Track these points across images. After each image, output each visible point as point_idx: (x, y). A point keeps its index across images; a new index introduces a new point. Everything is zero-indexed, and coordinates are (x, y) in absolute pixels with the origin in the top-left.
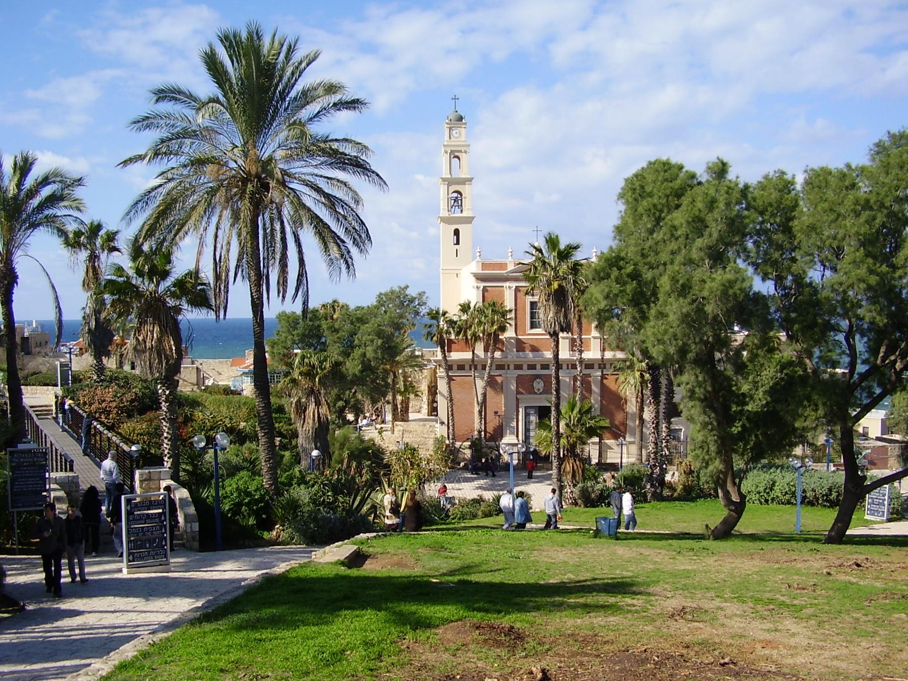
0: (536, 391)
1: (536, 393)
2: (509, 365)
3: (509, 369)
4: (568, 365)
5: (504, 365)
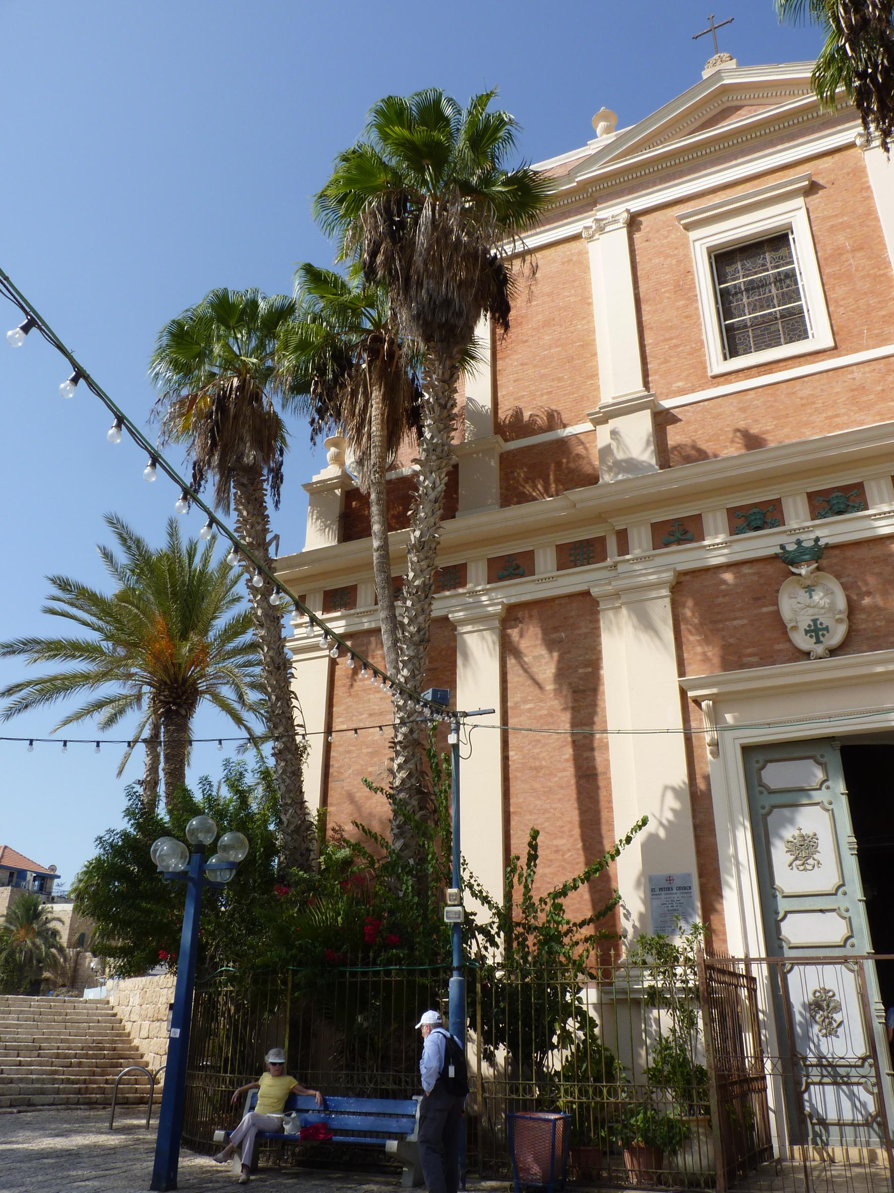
0: (803, 642)
1: (807, 655)
2: (623, 537)
3: (623, 549)
5: (602, 540)
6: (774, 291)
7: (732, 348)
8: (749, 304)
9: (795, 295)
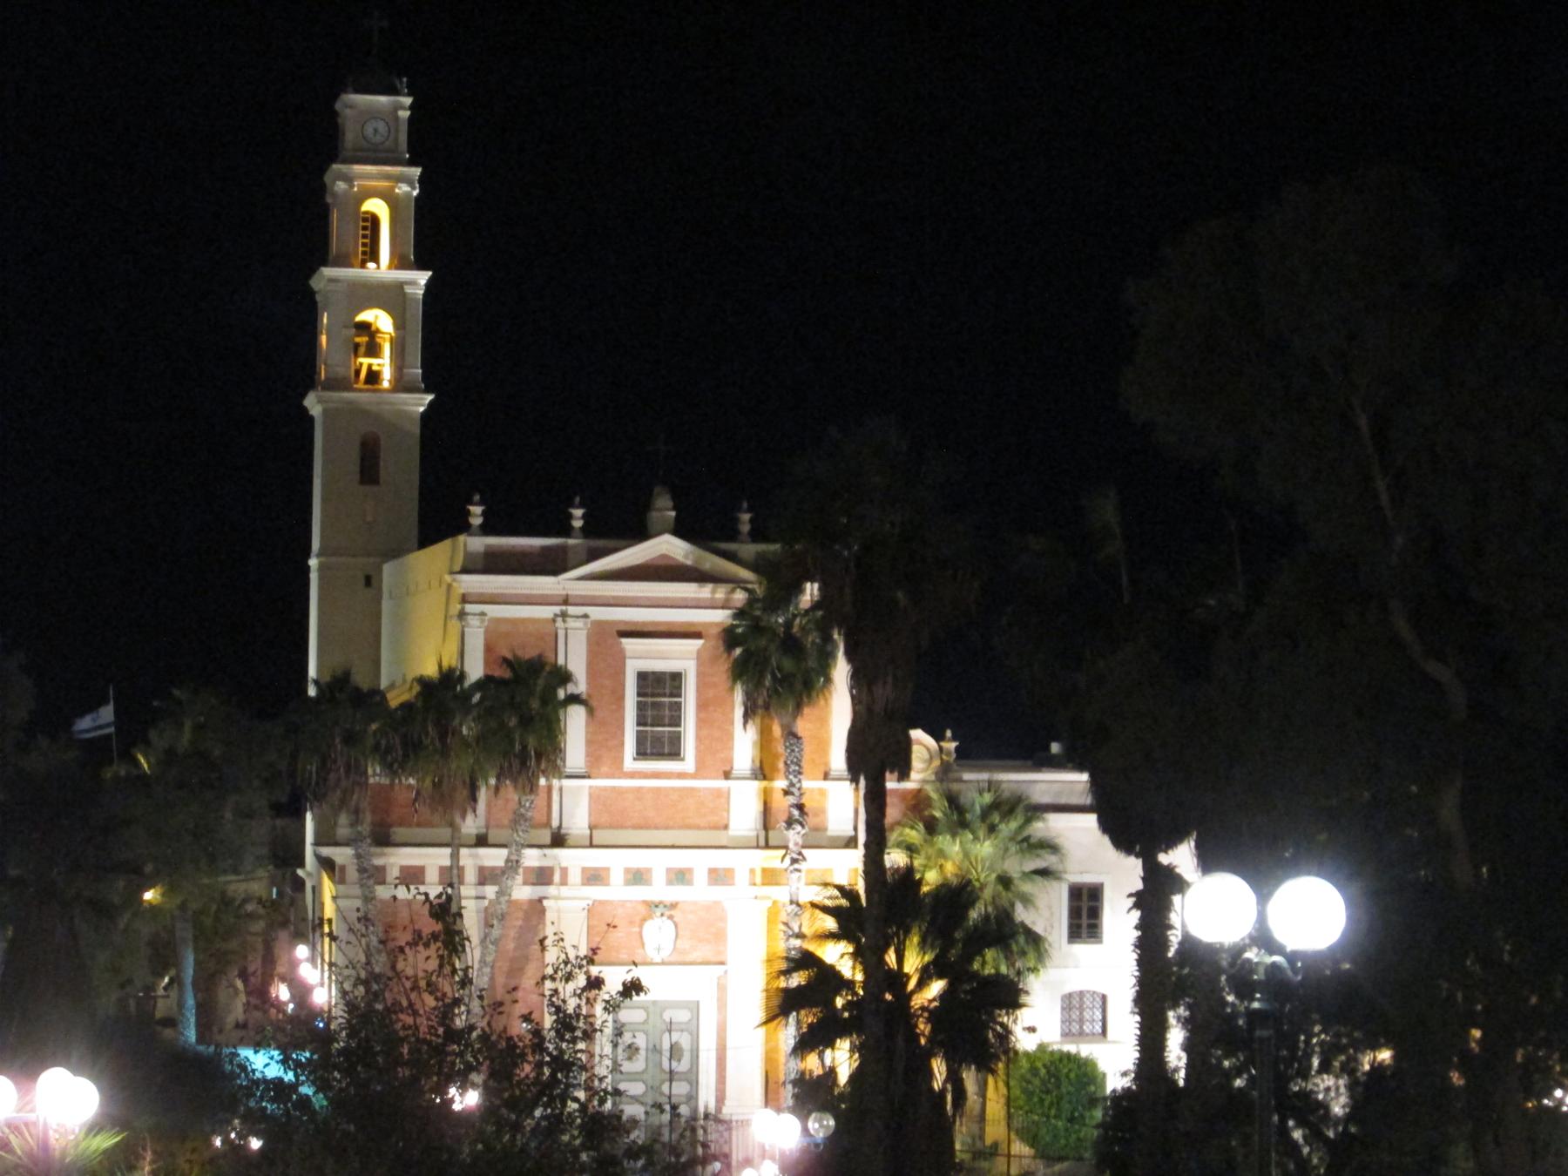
2: (564, 871)
4: (752, 871)
6: (667, 712)
7: (641, 754)
8: (652, 715)
9: (676, 721)
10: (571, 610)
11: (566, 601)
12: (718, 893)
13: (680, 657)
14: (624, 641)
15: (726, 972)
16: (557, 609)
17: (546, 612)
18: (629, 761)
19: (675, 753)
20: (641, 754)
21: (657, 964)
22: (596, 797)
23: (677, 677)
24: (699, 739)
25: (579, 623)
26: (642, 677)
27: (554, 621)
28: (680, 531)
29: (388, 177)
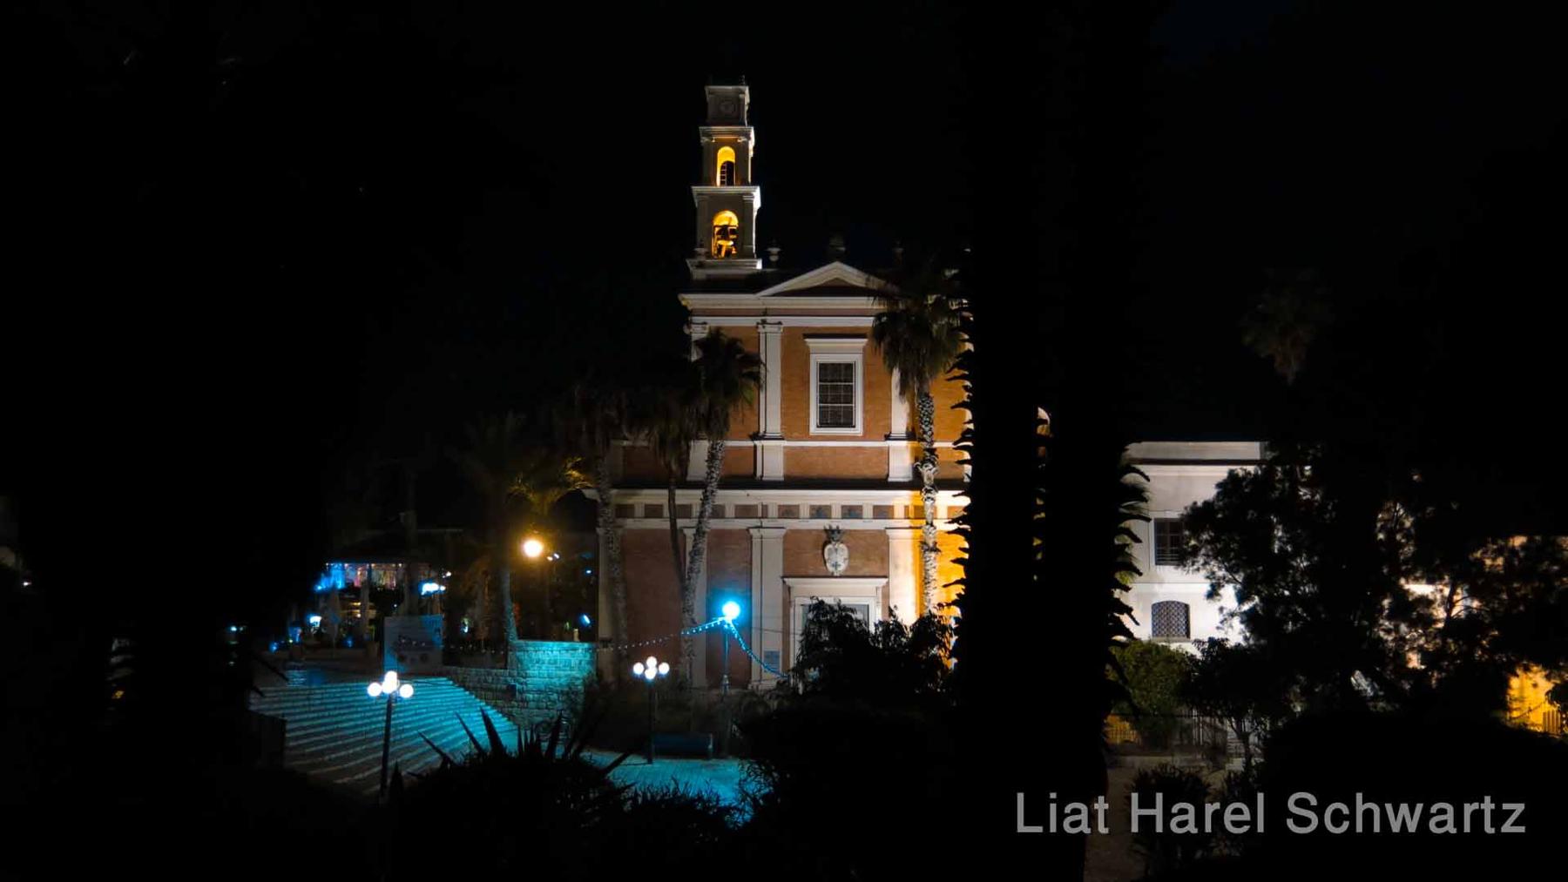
0: (831, 569)
5: (757, 506)
7: (823, 423)
9: (849, 399)
10: (769, 319)
11: (765, 313)
12: (880, 524)
13: (851, 352)
14: (807, 340)
15: (888, 583)
16: (759, 319)
17: (750, 322)
18: (813, 429)
19: (849, 424)
20: (823, 423)
21: (836, 577)
22: (790, 454)
23: (849, 367)
24: (865, 411)
25: (775, 329)
26: (823, 368)
27: (757, 327)
28: (848, 260)
29: (733, 133)
